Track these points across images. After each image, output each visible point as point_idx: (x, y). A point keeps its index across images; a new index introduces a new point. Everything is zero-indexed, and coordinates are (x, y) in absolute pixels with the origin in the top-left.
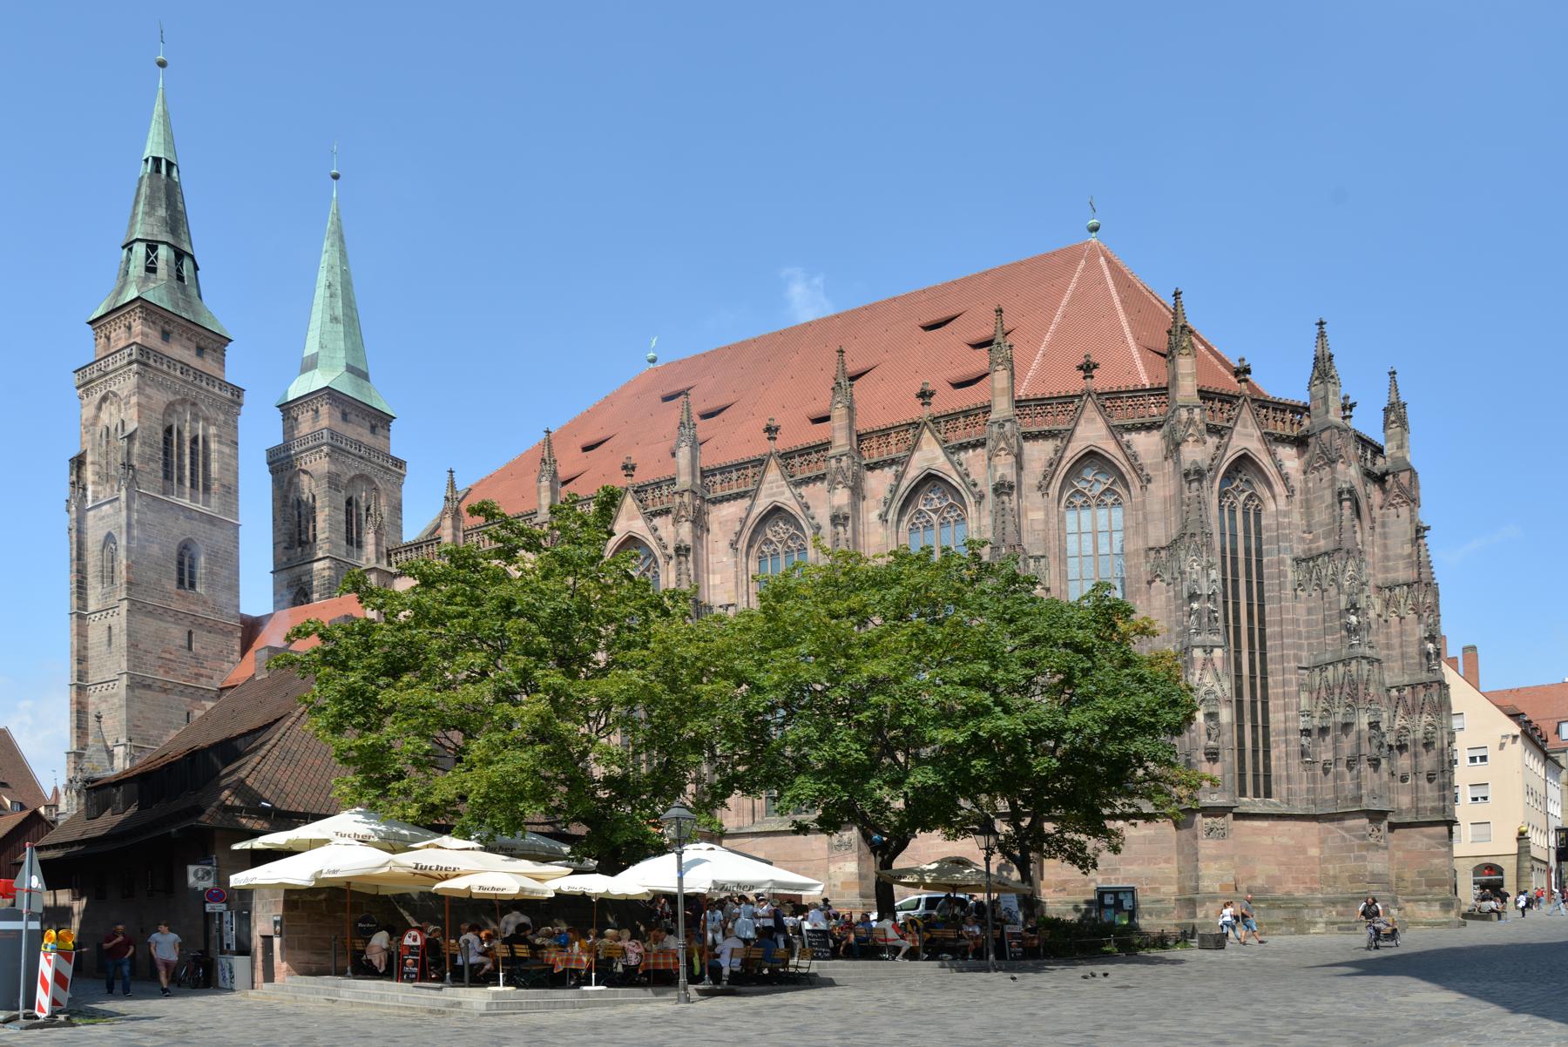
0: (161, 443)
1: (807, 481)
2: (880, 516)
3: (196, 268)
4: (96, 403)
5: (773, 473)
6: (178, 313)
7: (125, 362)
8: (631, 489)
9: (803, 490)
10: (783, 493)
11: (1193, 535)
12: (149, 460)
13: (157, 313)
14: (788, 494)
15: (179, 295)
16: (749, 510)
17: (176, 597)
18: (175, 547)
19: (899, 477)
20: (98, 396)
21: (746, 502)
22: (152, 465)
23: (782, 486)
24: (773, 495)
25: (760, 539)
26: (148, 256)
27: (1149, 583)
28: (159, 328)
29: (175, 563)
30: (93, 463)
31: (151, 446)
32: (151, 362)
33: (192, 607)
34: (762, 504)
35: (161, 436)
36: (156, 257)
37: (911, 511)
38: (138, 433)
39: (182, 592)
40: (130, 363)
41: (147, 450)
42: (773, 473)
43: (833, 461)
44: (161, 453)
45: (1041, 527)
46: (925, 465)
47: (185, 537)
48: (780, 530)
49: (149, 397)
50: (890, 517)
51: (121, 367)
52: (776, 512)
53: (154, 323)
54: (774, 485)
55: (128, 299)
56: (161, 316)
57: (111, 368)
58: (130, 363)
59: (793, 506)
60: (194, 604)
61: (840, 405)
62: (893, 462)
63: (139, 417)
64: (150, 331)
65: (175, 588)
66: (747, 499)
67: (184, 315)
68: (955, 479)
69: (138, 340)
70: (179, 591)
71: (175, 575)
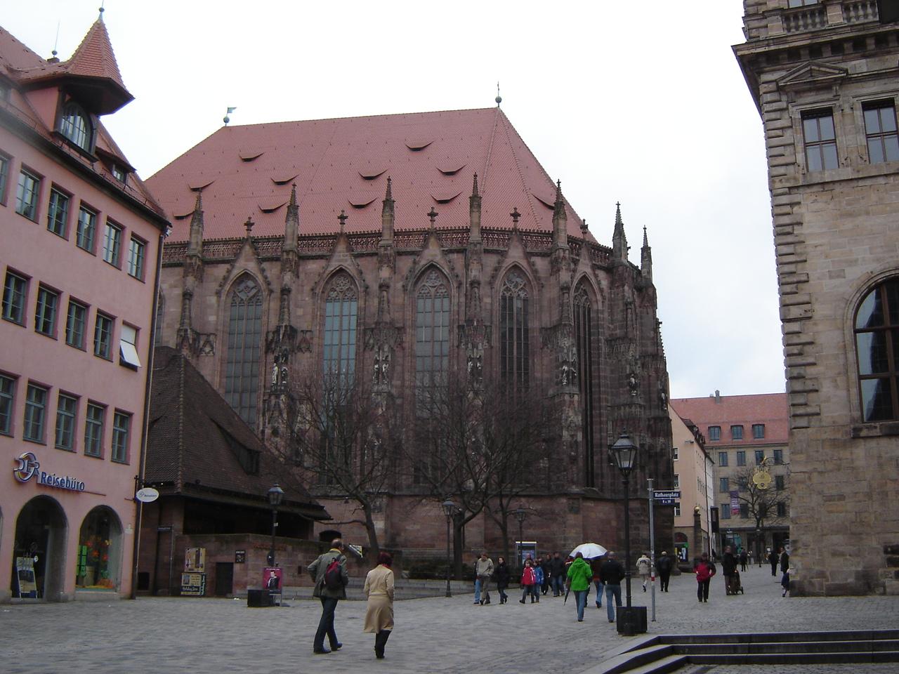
1: (361, 255)
2: (403, 286)
5: (341, 247)
8: (250, 240)
9: (359, 261)
10: (346, 261)
11: (565, 325)
14: (349, 262)
16: (325, 268)
19: (415, 263)
21: (323, 263)
23: (347, 256)
24: (339, 261)
25: (329, 287)
27: (542, 349)
34: (334, 265)
37: (420, 285)
42: (341, 247)
43: (382, 249)
45: (488, 307)
46: (430, 258)
48: (342, 283)
50: (409, 288)
52: (341, 272)
54: (341, 254)
59: (352, 270)
61: (387, 214)
62: (412, 253)
66: (323, 261)
68: (446, 271)
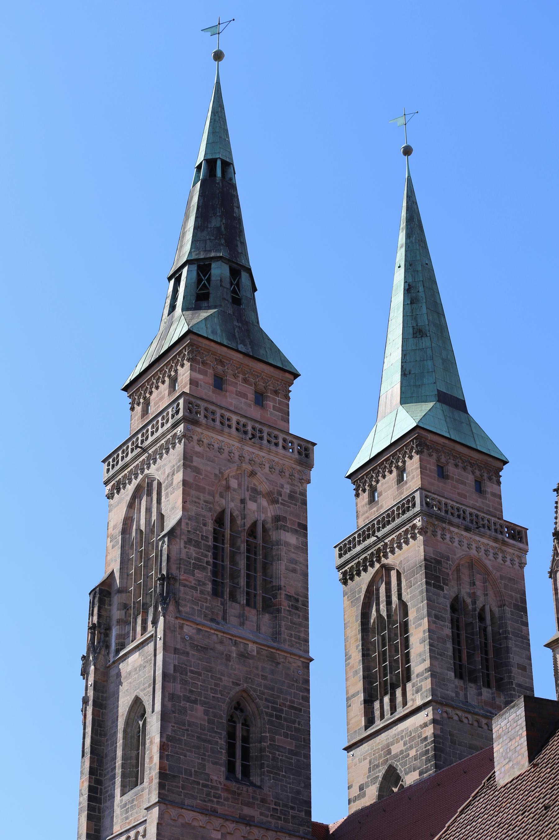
0: (211, 537)
3: (255, 289)
4: (128, 498)
6: (233, 346)
7: (169, 425)
12: (196, 566)
13: (208, 351)
15: (236, 323)
17: (224, 795)
18: (224, 706)
20: (130, 488)
22: (199, 574)
26: (199, 280)
28: (210, 371)
29: (224, 733)
30: (120, 591)
31: (197, 545)
32: (201, 417)
33: (247, 811)
35: (210, 527)
36: (209, 280)
38: (183, 526)
39: (233, 786)
40: (175, 426)
41: (193, 551)
44: (210, 554)
47: (238, 689)
49: (197, 470)
51: (164, 435)
53: (204, 363)
55: (175, 339)
56: (214, 353)
57: (151, 439)
58: (175, 426)
60: (248, 804)
63: (184, 502)
64: (201, 377)
65: (222, 779)
67: (241, 347)
69: (187, 390)
70: (228, 783)
71: (224, 758)
